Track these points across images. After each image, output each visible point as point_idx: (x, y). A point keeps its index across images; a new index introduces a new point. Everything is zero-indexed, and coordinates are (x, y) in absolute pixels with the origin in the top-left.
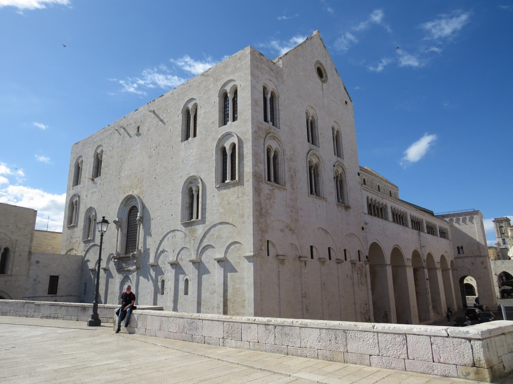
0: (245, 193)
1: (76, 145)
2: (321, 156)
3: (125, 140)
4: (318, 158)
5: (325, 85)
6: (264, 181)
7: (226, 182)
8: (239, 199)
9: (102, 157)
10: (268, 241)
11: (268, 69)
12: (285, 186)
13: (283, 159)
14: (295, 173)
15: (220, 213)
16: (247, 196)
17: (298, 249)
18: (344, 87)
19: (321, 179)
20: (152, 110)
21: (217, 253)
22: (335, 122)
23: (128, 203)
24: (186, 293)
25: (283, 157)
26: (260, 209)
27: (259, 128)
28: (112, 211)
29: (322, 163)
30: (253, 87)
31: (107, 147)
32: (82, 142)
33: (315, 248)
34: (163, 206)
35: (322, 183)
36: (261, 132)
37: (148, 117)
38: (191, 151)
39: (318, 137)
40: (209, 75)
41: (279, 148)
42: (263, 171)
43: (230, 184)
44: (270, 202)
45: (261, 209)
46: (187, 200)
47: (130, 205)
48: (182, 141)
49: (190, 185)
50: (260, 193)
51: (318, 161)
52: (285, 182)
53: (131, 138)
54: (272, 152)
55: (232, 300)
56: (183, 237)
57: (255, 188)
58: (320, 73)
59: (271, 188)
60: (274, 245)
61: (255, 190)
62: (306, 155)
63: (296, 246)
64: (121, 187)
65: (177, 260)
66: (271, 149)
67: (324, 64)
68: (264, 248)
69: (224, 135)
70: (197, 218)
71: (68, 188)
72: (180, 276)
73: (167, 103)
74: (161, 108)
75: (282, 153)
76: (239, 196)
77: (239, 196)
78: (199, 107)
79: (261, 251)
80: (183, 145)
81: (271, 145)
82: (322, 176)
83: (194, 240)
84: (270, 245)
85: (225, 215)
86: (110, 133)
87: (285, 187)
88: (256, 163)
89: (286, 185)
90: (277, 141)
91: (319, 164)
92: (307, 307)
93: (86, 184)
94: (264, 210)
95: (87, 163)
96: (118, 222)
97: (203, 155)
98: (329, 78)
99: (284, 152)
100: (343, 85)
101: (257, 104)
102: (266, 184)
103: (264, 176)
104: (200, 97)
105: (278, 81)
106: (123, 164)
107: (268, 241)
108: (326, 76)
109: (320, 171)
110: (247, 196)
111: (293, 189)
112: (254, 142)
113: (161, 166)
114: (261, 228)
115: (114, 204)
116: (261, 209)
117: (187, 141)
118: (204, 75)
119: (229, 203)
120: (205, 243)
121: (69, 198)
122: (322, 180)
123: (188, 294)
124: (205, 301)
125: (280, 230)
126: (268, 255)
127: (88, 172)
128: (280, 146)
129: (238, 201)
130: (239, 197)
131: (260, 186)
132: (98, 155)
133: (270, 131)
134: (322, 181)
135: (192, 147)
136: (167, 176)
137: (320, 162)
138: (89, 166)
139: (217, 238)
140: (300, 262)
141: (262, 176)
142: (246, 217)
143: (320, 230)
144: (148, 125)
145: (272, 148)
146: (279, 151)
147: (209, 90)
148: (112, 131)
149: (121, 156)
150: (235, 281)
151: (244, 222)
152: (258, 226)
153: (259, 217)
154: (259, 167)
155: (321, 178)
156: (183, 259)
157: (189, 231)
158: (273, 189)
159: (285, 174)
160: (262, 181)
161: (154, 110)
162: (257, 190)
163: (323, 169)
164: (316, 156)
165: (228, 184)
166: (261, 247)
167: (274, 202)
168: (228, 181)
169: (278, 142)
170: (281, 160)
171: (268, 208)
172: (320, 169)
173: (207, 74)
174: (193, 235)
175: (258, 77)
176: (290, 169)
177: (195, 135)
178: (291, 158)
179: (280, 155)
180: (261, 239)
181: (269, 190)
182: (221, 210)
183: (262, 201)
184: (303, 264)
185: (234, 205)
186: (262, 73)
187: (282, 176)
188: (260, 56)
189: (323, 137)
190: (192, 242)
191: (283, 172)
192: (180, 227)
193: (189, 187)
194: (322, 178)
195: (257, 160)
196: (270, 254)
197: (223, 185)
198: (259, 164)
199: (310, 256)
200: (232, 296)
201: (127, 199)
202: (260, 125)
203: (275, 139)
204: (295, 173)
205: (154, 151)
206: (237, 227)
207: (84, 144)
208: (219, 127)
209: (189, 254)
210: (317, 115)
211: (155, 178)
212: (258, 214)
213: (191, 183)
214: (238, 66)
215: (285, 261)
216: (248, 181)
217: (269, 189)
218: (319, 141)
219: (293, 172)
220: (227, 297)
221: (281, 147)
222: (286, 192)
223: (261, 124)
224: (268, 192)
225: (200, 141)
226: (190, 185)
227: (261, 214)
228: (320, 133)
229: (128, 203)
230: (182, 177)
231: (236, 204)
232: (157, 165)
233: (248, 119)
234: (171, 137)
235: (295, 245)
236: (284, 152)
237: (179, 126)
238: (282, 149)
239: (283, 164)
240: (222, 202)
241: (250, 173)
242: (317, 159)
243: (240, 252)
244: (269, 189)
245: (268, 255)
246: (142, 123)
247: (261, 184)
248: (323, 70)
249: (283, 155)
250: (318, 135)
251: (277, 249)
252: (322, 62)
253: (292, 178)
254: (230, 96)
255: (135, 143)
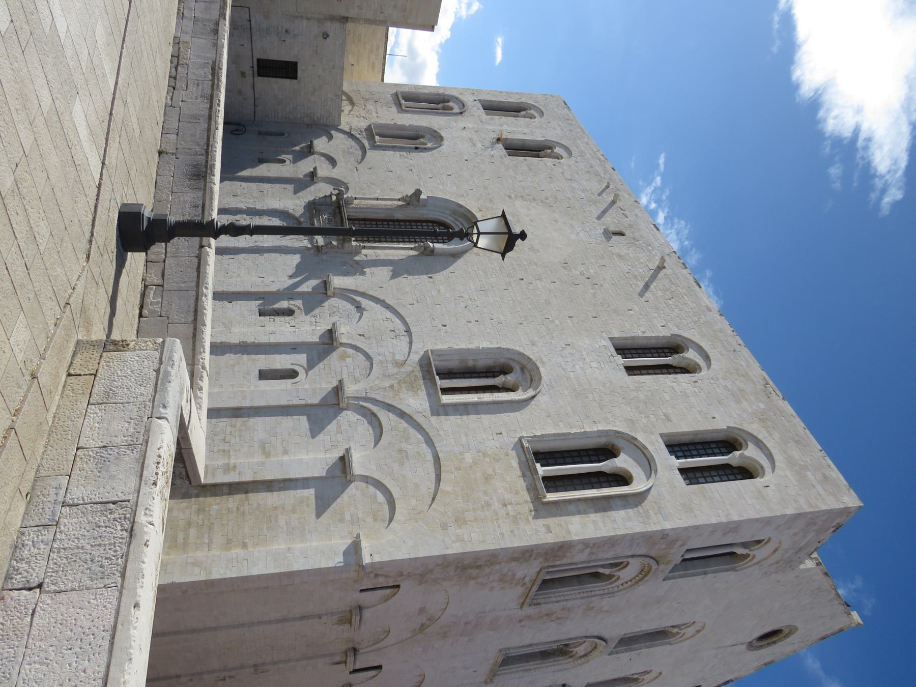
0: (519, 524)
1: (563, 104)
2: (589, 661)
3: (591, 205)
4: (585, 655)
5: (744, 647)
6: (546, 564)
7: (538, 465)
8: (501, 506)
9: (549, 156)
10: (398, 586)
11: (802, 544)
12: (530, 605)
13: (593, 593)
14: (558, 619)
15: (462, 453)
16: (512, 531)
17: (374, 644)
18: (732, 681)
19: (537, 664)
20: (665, 264)
21: (362, 454)
22: (661, 673)
23: (460, 219)
24: (264, 375)
25: (597, 593)
26: (478, 564)
27: (673, 542)
28: (438, 185)
29: (572, 664)
30: (767, 522)
31: (570, 166)
32: (570, 115)
33: (377, 675)
34: (463, 302)
35: (528, 668)
36: (663, 546)
37: (648, 254)
38: (594, 365)
39: (632, 650)
40: (769, 397)
41: (619, 582)
42: (569, 561)
43: (535, 476)
44: (494, 581)
45: (479, 567)
46: (483, 362)
47: (455, 224)
48: (611, 339)
49: (517, 368)
50: (518, 560)
51: (578, 655)
52: (539, 604)
53: (597, 218)
54: (610, 570)
55: (247, 508)
56: (396, 358)
57: (532, 551)
58: (771, 636)
59: (527, 579)
60: (386, 599)
61: (527, 551)
62: (595, 634)
63: (383, 639)
64: (491, 201)
65: (342, 344)
66: (617, 568)
67: (789, 640)
68: (381, 581)
69: (645, 451)
70: (446, 391)
71: (476, 90)
72: (305, 356)
73: (686, 297)
74: (672, 283)
75: (606, 591)
76: (509, 507)
77: (509, 507)
78: (694, 379)
79: (372, 575)
80: (604, 343)
81: (628, 567)
82: (542, 667)
83: (392, 387)
84: (388, 591)
85: (458, 469)
86: (598, 172)
87: (526, 605)
88: (592, 545)
89: (531, 607)
90: (637, 578)
91: (571, 657)
92: (230, 677)
93: (488, 127)
94: (474, 572)
95: (530, 126)
96: (419, 200)
97: (591, 397)
98: (756, 652)
99: (609, 593)
100: (736, 679)
101: (728, 532)
102: (538, 569)
103: (558, 563)
104: (718, 379)
105: (771, 565)
106: (541, 204)
107: (398, 586)
108: (761, 647)
109: (556, 661)
110: (511, 531)
111: (520, 621)
112: (643, 536)
113: (550, 290)
114: (431, 571)
115: (455, 188)
116: (479, 567)
117: (615, 353)
118: (767, 386)
119: (487, 478)
120: (388, 418)
121: (455, 93)
122: (535, 669)
123: (260, 379)
124: (243, 428)
125: (425, 607)
126: (362, 591)
127: (513, 129)
128: (622, 585)
129: (496, 505)
130: (505, 505)
131: (535, 559)
132: (550, 148)
133: (663, 564)
134: (532, 667)
135: (603, 366)
136: (530, 309)
137: (577, 660)
138: (525, 131)
139: (400, 451)
140: (342, 652)
141: (559, 560)
142: (459, 531)
143: (421, 679)
144: (631, 255)
145: (620, 570)
146: (611, 583)
147: (738, 402)
148: (603, 176)
149: (556, 198)
150: (294, 511)
151: (444, 527)
152: (437, 565)
153: (460, 565)
154: (582, 551)
155: (538, 666)
156: (345, 360)
157: (413, 371)
158: (524, 584)
159: (558, 602)
160: (546, 560)
161: (664, 268)
162: (525, 554)
163: (560, 667)
164: (591, 652)
165: (533, 474)
166: (381, 575)
167: (492, 589)
168: (542, 470)
169: (634, 581)
170: (592, 589)
171: (480, 580)
172: (559, 660)
173: (771, 393)
174: (403, 385)
175: (788, 528)
176: (569, 609)
177: (631, 370)
178: (593, 608)
179: (602, 586)
180: (404, 573)
181: (523, 576)
182: (468, 458)
183: (497, 567)
184: (338, 659)
185: (485, 493)
186: (795, 534)
187: (552, 595)
188: (833, 527)
189: (631, 659)
190: (387, 384)
191: (563, 598)
192: (420, 348)
193: (513, 364)
194: (539, 668)
195: (599, 547)
196: (364, 594)
197: (528, 457)
198: (588, 551)
199: (358, 667)
200: (255, 505)
201: (469, 216)
202: (680, 543)
203: (641, 574)
204: (558, 619)
205: (579, 273)
206: (433, 505)
207: (568, 119)
208: (662, 435)
209: (357, 375)
210: (681, 641)
211: (521, 278)
212: (465, 563)
213: (523, 369)
214: (809, 474)
215: (347, 626)
216: (549, 530)
217: (525, 577)
218: (622, 652)
219: (559, 616)
220: (253, 491)
221: (621, 587)
222: (515, 609)
223: (681, 546)
224: (519, 574)
225: (621, 386)
226: (517, 368)
227: (465, 568)
228: (641, 652)
229: (460, 219)
230: (533, 345)
231: (487, 498)
232: (550, 282)
233: (695, 516)
234: (615, 311)
235: (385, 638)
236: (609, 593)
237: (642, 329)
238: (616, 589)
239: (582, 595)
240: (487, 459)
241: (569, 532)
242: (583, 653)
243: (370, 520)
244: (525, 577)
245: (362, 591)
246: (633, 241)
247: (541, 560)
248: (774, 639)
249: (601, 592)
250: (635, 650)
251: (377, 605)
252: (792, 637)
253: (547, 615)
254: (733, 458)
255: (588, 229)
